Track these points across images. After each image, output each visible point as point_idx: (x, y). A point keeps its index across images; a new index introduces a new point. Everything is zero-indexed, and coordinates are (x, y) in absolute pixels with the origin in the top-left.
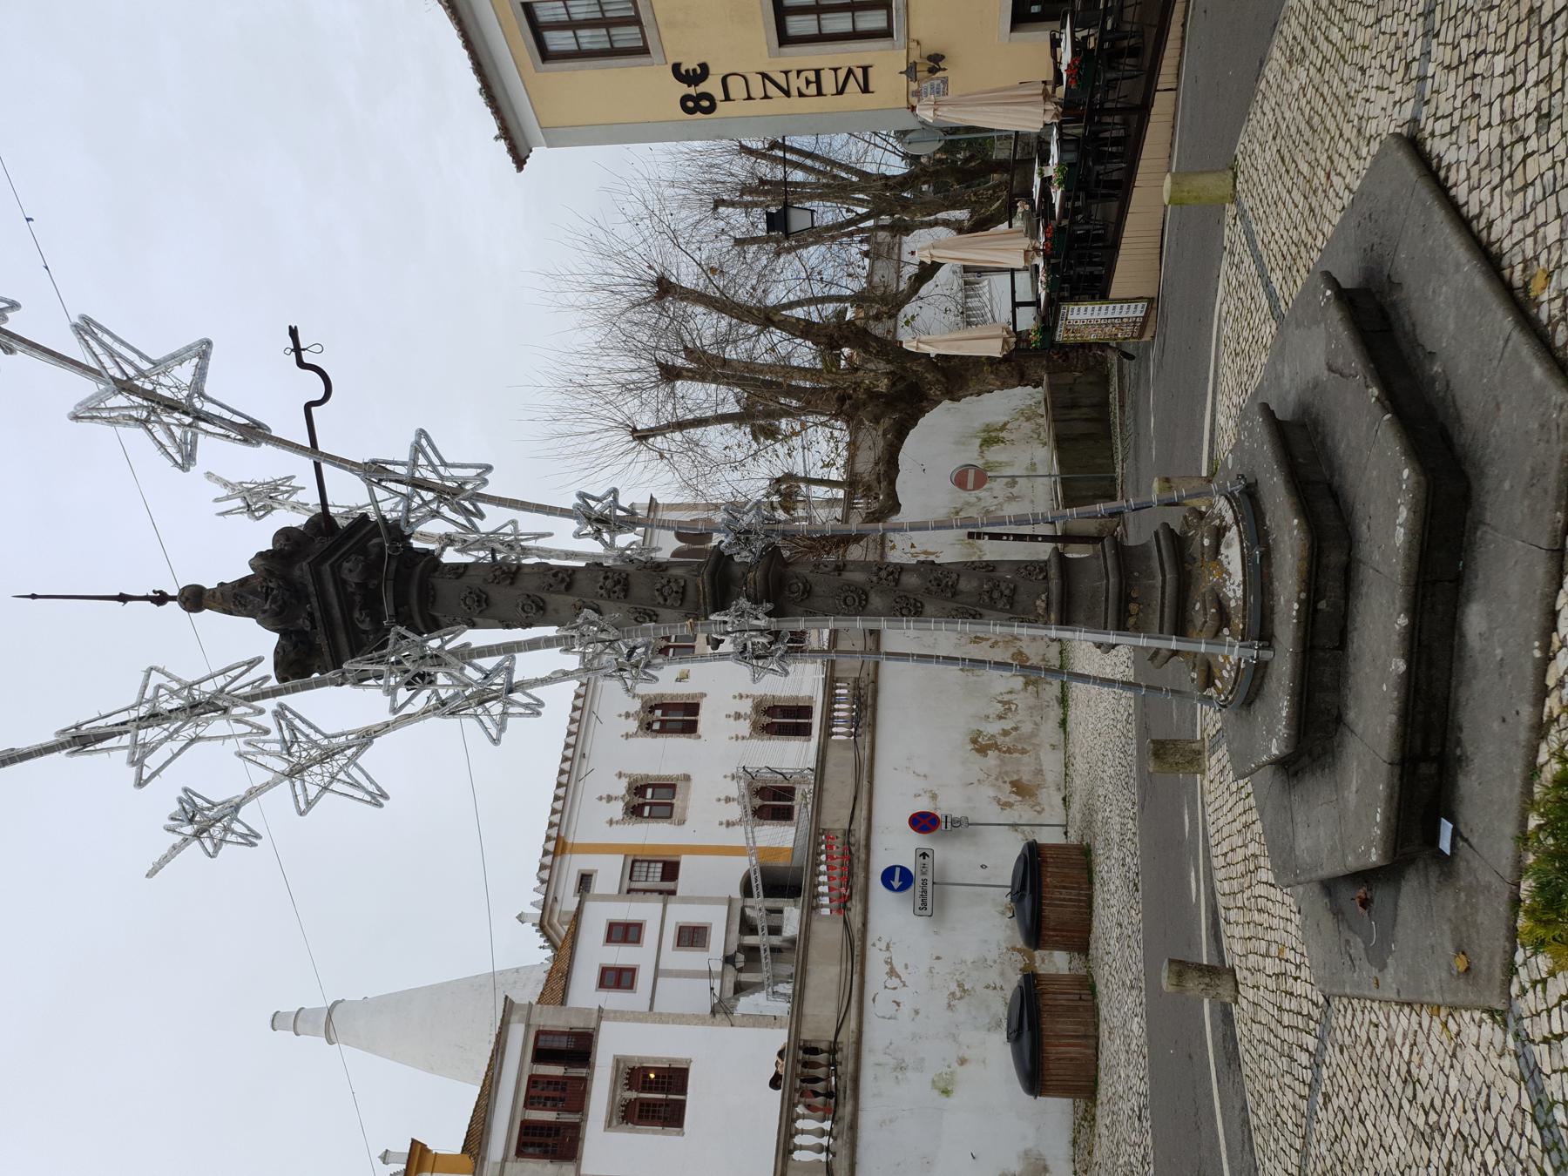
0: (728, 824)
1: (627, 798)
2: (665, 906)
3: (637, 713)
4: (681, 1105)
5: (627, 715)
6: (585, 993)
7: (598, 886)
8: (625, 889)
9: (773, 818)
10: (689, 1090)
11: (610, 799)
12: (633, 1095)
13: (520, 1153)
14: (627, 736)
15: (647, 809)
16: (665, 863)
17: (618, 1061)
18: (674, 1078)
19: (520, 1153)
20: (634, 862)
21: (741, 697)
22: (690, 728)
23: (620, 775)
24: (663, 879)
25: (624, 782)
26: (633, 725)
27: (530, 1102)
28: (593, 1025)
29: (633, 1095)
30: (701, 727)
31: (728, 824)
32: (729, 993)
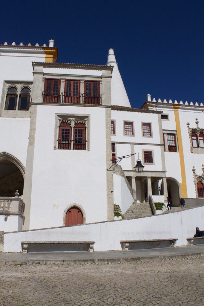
0: (194, 170)
1: (198, 129)
2: (159, 145)
7: (164, 121)
8: (164, 132)
9: (198, 189)
11: (197, 123)
12: (73, 124)
13: (47, 80)
15: (195, 138)
16: (175, 146)
20: (174, 135)
24: (169, 146)
28: (103, 104)
31: (194, 170)
32: (127, 174)
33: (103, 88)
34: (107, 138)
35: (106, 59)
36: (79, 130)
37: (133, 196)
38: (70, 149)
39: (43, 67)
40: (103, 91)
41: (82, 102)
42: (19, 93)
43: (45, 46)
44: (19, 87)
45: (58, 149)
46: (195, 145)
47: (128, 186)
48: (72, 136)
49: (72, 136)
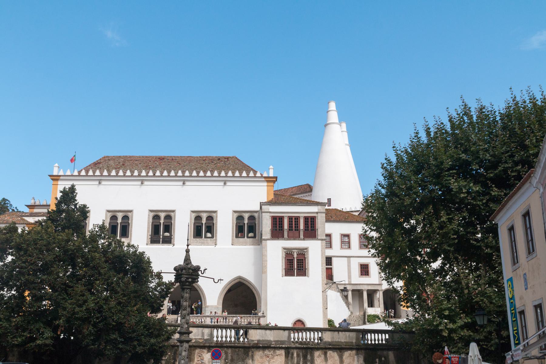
4: (293, 275)
6: (336, 229)
10: (298, 277)
27: (290, 218)
28: (319, 238)
29: (295, 256)
33: (319, 223)
34: (322, 266)
35: (326, 118)
36: (300, 260)
37: (349, 309)
38: (294, 276)
39: (269, 206)
40: (319, 225)
41: (302, 237)
42: (246, 222)
43: (265, 175)
44: (246, 216)
45: (286, 275)
47: (343, 300)
48: (295, 265)
49: (295, 265)
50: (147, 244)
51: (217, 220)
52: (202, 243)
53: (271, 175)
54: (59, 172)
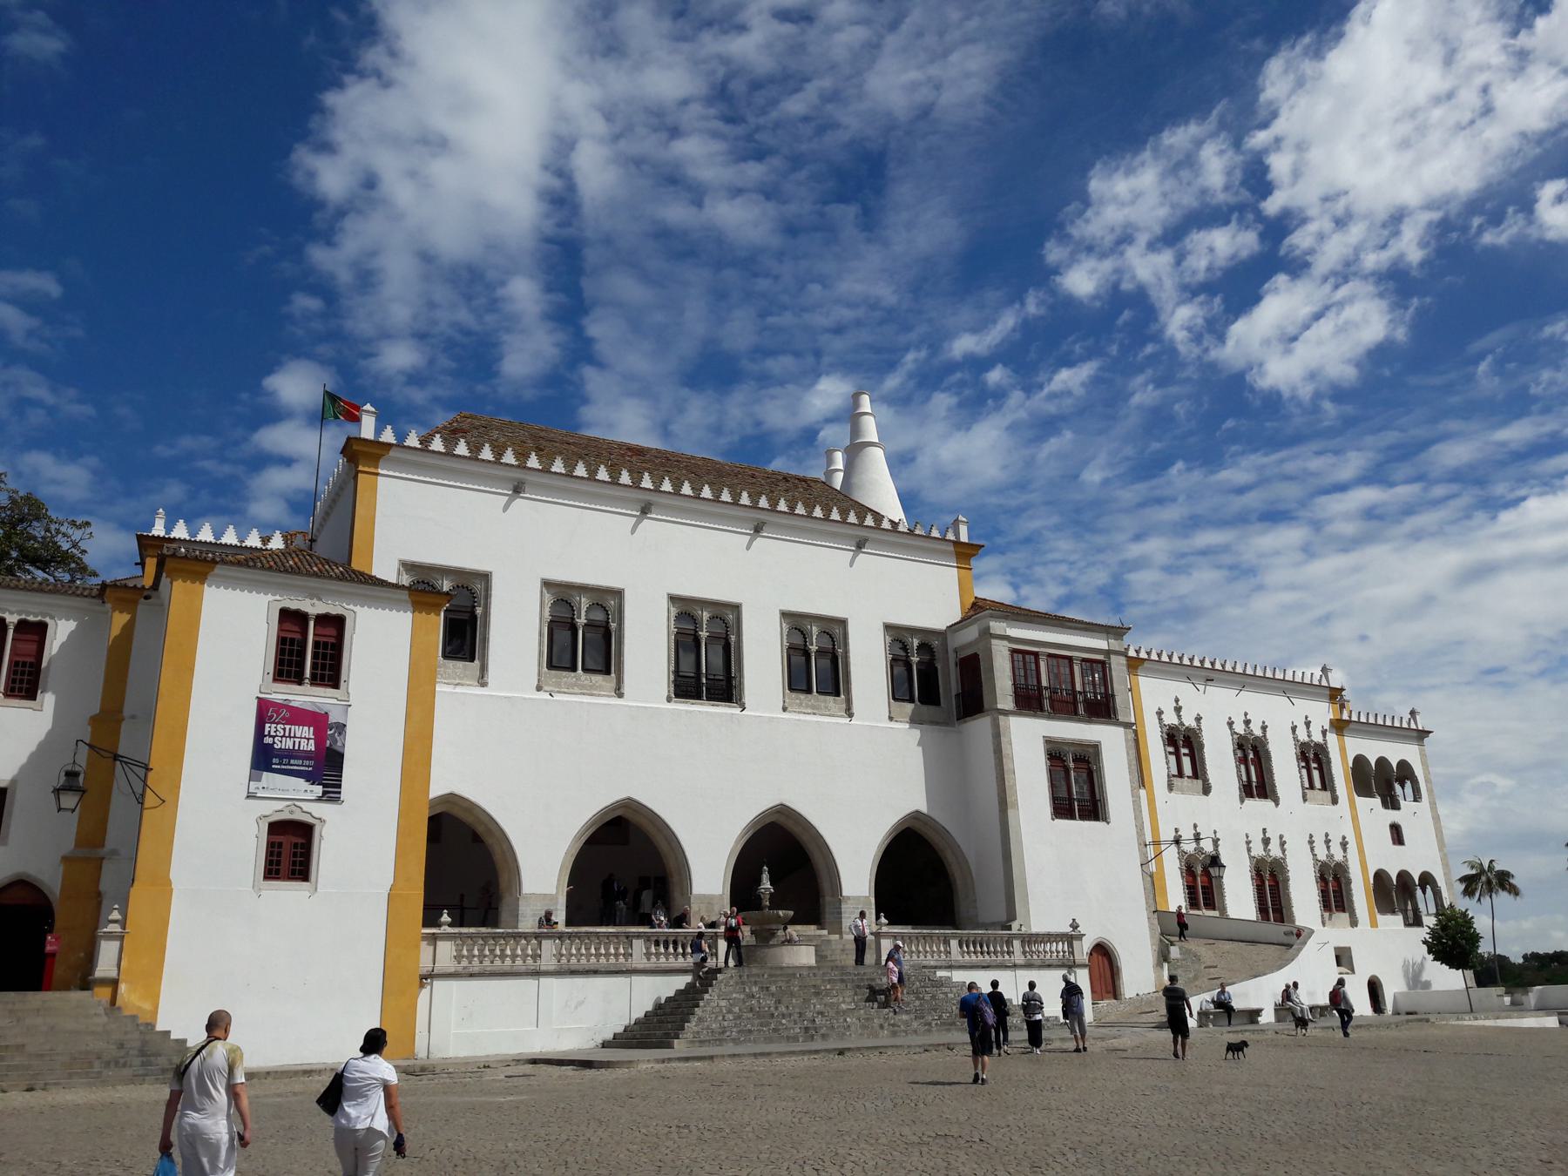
3: (1251, 733)
5: (1247, 722)
11: (1178, 710)
13: (1014, 651)
14: (1230, 724)
15: (1171, 749)
17: (1096, 748)
18: (1093, 809)
19: (1014, 651)
21: (1283, 844)
22: (1247, 791)
23: (1198, 719)
25: (1194, 724)
26: (1240, 728)
28: (1121, 719)
29: (1072, 765)
30: (1249, 802)
38: (1072, 817)
46: (1174, 771)
49: (1077, 791)
50: (669, 700)
51: (846, 644)
52: (813, 707)
53: (964, 538)
54: (379, 430)
